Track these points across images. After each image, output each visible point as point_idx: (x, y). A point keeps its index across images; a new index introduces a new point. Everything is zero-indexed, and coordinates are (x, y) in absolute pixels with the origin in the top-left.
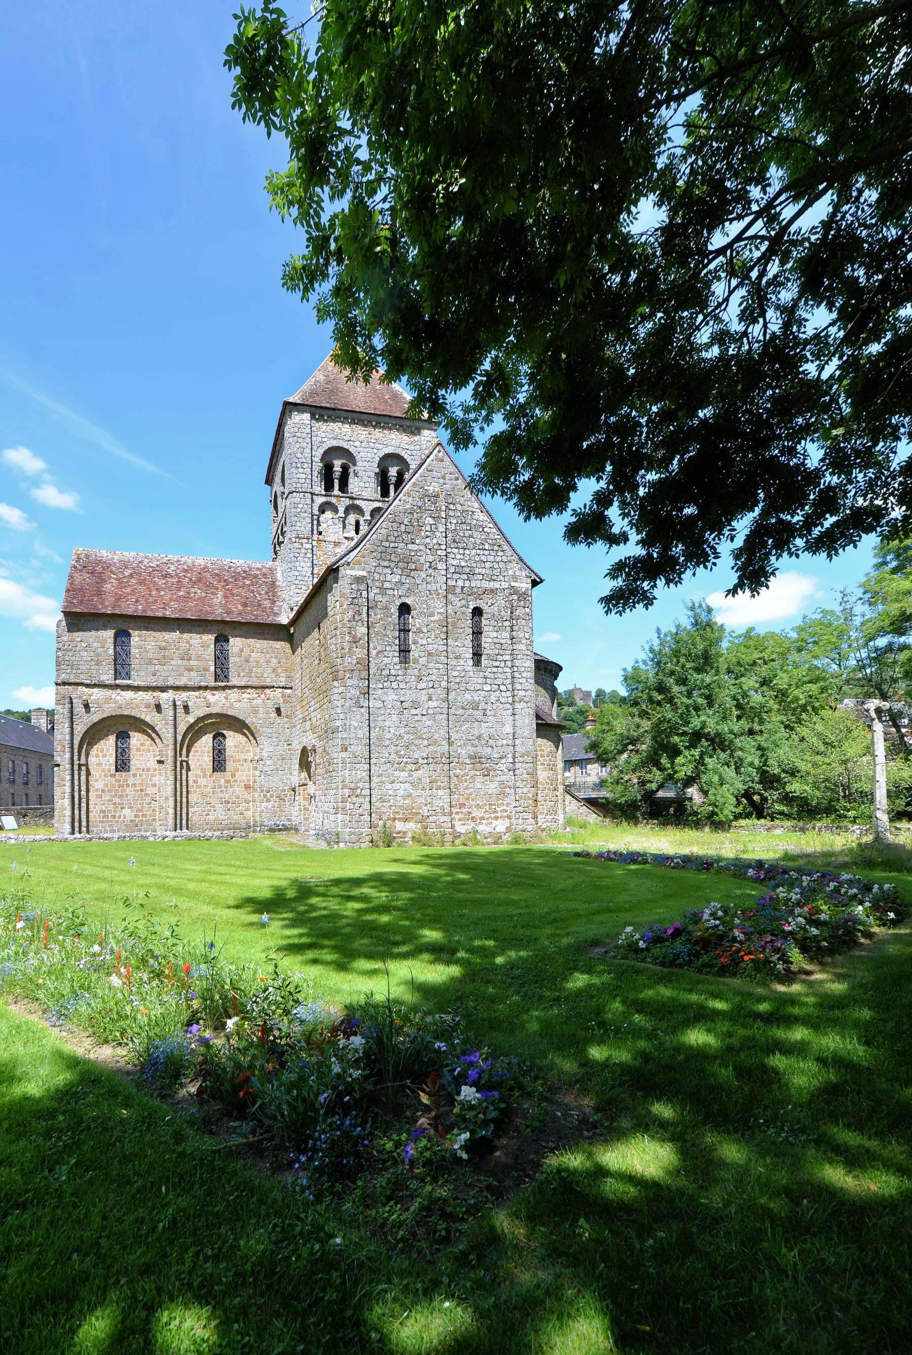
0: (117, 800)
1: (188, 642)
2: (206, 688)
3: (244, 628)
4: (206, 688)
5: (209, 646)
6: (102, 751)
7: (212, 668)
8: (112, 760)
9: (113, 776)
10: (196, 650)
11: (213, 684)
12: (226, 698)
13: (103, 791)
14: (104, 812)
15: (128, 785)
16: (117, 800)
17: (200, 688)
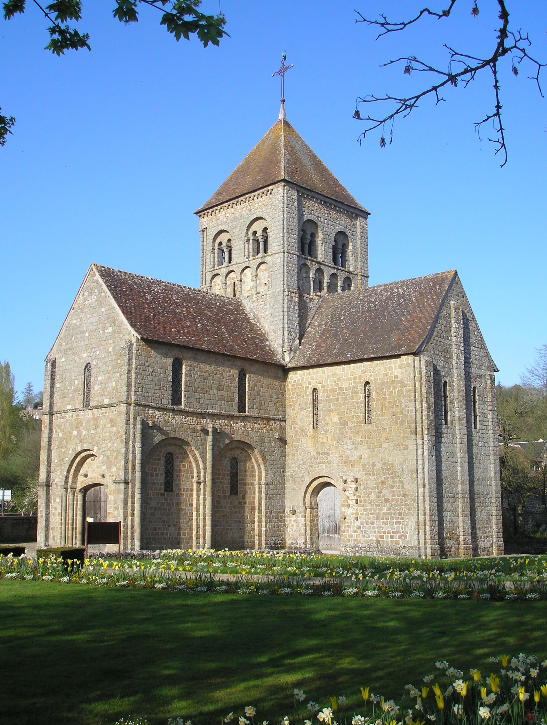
0: (165, 518)
1: (222, 375)
2: (232, 417)
3: (257, 366)
4: (232, 417)
5: (234, 380)
6: (155, 471)
7: (237, 399)
8: (162, 479)
9: (163, 495)
10: (226, 382)
11: (237, 414)
12: (244, 427)
13: (156, 509)
14: (155, 529)
15: (173, 504)
16: (165, 518)
17: (228, 416)
